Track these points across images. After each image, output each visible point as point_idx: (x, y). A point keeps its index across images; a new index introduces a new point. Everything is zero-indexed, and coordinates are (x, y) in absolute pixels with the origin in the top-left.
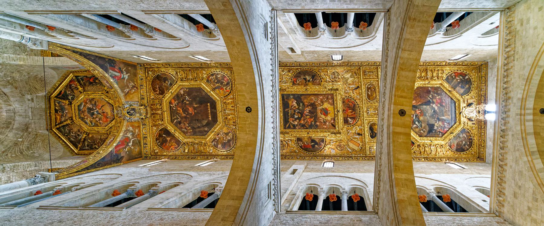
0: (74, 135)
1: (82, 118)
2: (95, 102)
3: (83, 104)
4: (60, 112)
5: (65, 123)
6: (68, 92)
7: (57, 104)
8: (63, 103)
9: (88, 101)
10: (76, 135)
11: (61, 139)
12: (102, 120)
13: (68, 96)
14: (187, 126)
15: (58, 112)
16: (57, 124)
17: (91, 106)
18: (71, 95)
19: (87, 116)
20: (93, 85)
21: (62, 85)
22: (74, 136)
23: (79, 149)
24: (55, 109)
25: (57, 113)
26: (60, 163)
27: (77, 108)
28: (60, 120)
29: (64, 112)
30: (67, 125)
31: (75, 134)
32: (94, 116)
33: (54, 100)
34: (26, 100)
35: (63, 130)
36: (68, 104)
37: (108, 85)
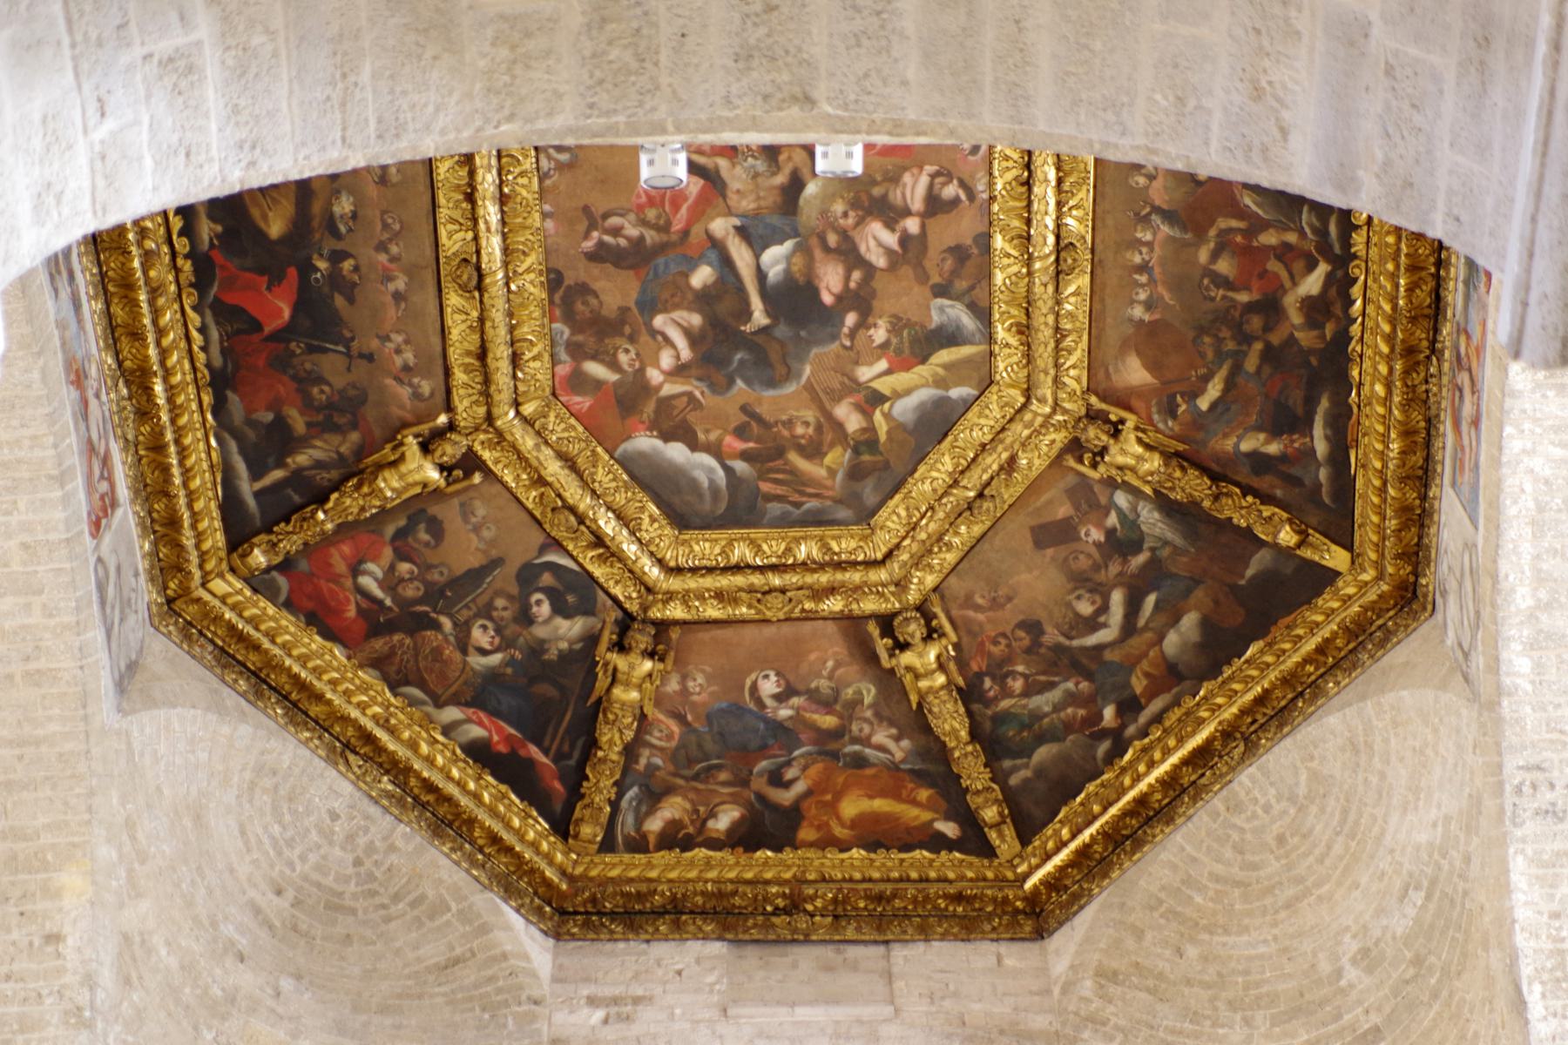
0: (1117, 598)
1: (856, 473)
2: (600, 255)
3: (645, 442)
4: (777, 779)
5: (951, 722)
7: (672, 809)
9: (595, 369)
10: (1121, 580)
12: (894, 179)
13: (537, 649)
15: (785, 797)
16: (949, 829)
18: (526, 617)
19: (819, 398)
20: (335, 279)
21: (380, 734)
22: (1133, 607)
23: (1337, 558)
24: (746, 838)
25: (793, 816)
26: (1540, 578)
27: (705, 547)
28: (893, 780)
29: (778, 727)
30: (969, 695)
31: (1101, 592)
32: (831, 280)
33: (608, 845)
35: (1043, 753)
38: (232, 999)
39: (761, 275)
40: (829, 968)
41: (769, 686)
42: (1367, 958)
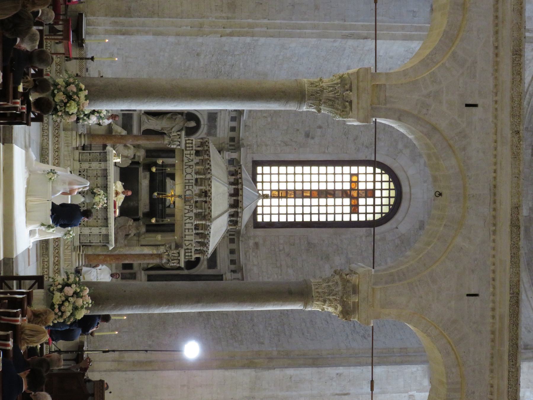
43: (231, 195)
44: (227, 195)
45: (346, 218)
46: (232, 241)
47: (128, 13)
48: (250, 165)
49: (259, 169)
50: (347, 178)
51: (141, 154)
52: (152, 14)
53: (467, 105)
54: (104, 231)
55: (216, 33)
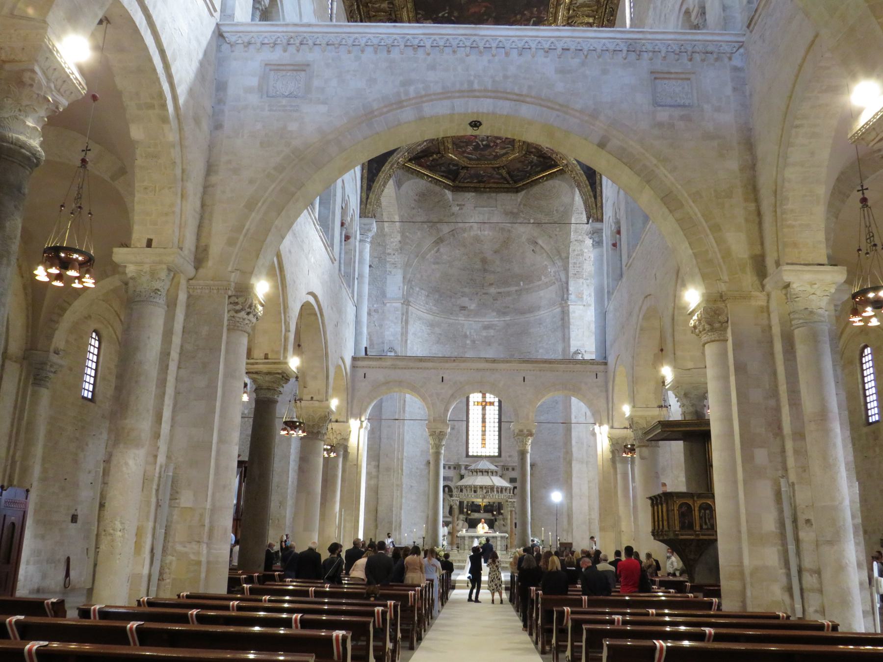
0: (530, 167)
2: (461, 142)
3: (465, 155)
6: (443, 169)
8: (465, 174)
11: (537, 179)
14: (521, 18)
17: (471, 148)
18: (449, 166)
24: (479, 182)
27: (474, 162)
30: (508, 173)
32: (492, 144)
34: (460, 212)
36: (467, 170)
37: (425, 143)
38: (413, 215)
39: (482, 144)
40: (488, 198)
41: (482, 172)
42: (556, 210)
43: (483, 475)
44: (482, 477)
45: (497, 408)
46: (508, 469)
47: (391, 523)
48: (468, 459)
49: (470, 454)
50: (476, 407)
51: (462, 517)
52: (392, 511)
53: (442, 381)
54: (499, 539)
55: (401, 478)
